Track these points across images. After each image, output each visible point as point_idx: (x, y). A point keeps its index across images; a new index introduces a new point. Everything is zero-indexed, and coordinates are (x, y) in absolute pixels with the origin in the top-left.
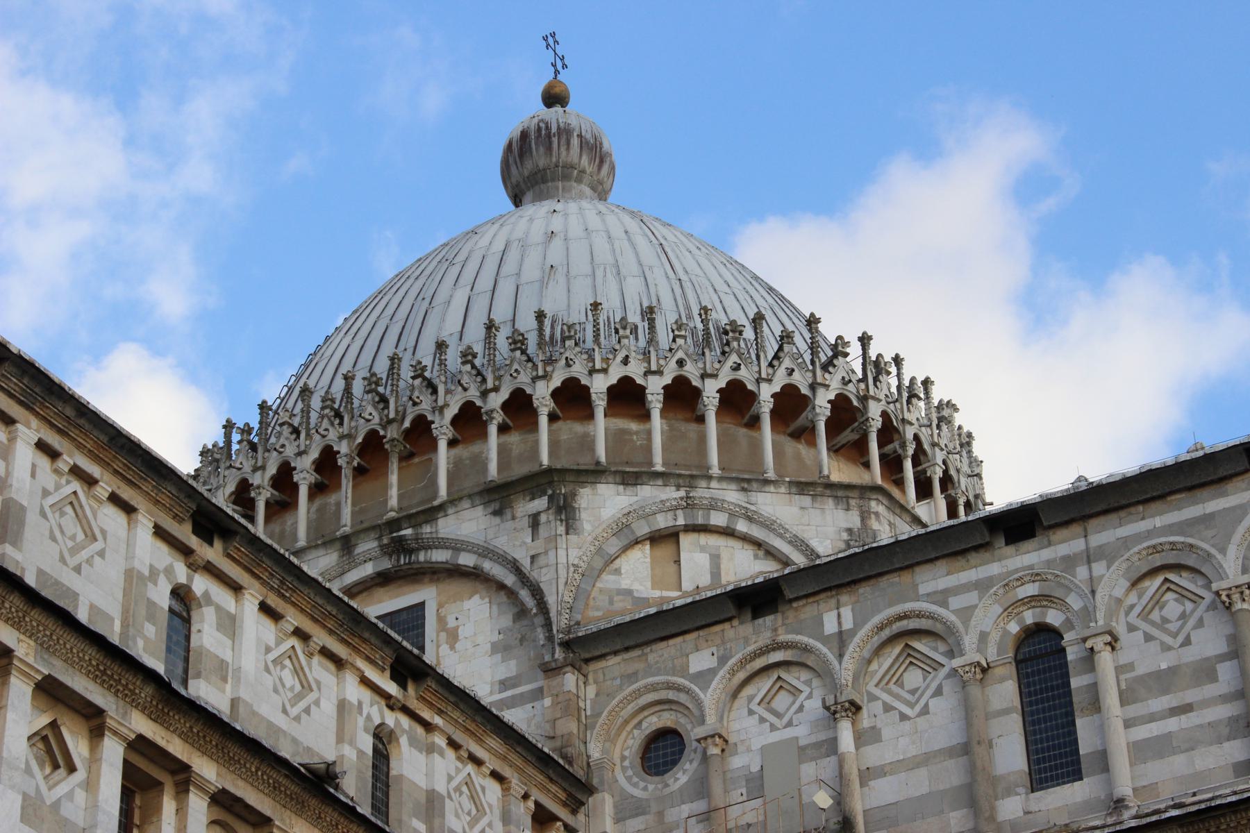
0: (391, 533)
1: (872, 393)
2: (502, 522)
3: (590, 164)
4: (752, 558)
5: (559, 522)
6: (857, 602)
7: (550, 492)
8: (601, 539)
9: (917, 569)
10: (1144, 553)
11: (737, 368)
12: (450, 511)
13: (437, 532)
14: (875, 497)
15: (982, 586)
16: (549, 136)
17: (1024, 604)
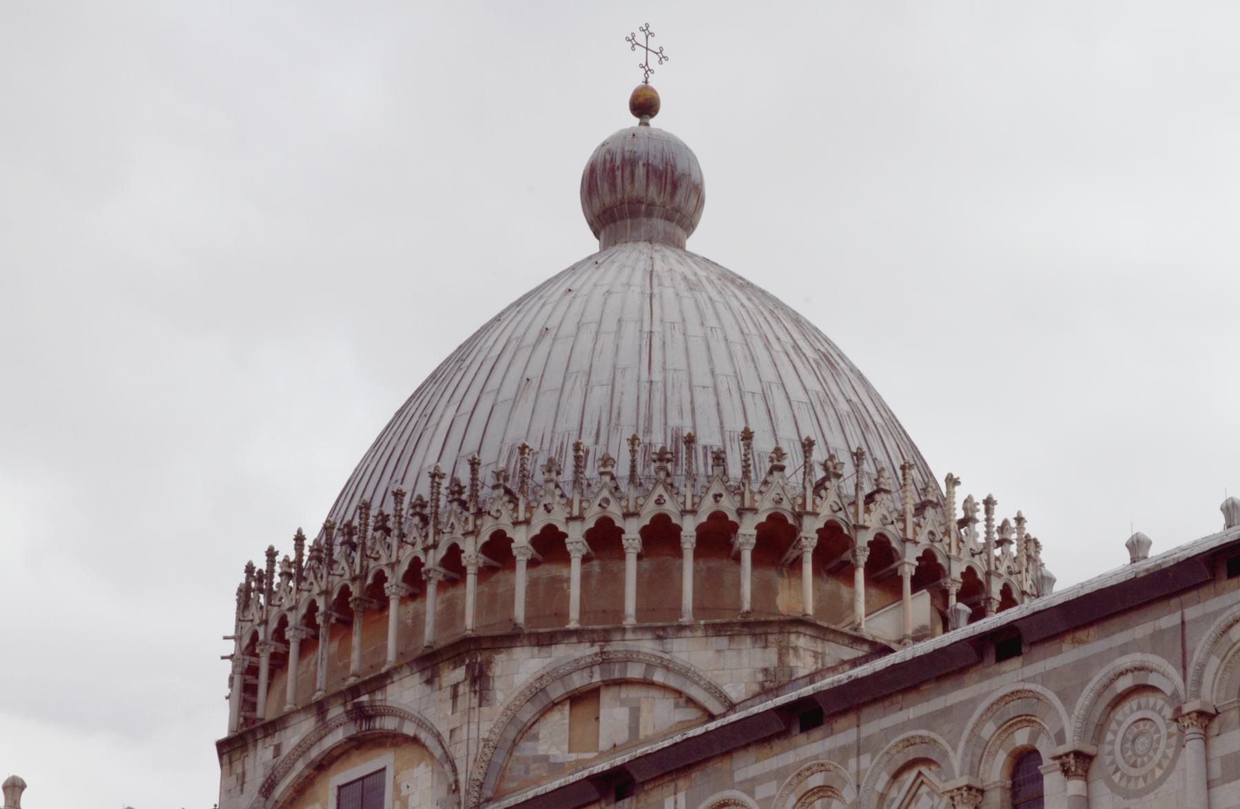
0: (353, 699)
1: (809, 508)
2: (432, 691)
3: (659, 194)
4: (672, 707)
5: (473, 694)
6: (690, 787)
7: (467, 661)
8: (513, 708)
9: (735, 755)
10: (901, 746)
11: (659, 502)
12: (396, 678)
13: (385, 699)
14: (794, 630)
15: (778, 775)
16: (613, 170)
17: (814, 794)
